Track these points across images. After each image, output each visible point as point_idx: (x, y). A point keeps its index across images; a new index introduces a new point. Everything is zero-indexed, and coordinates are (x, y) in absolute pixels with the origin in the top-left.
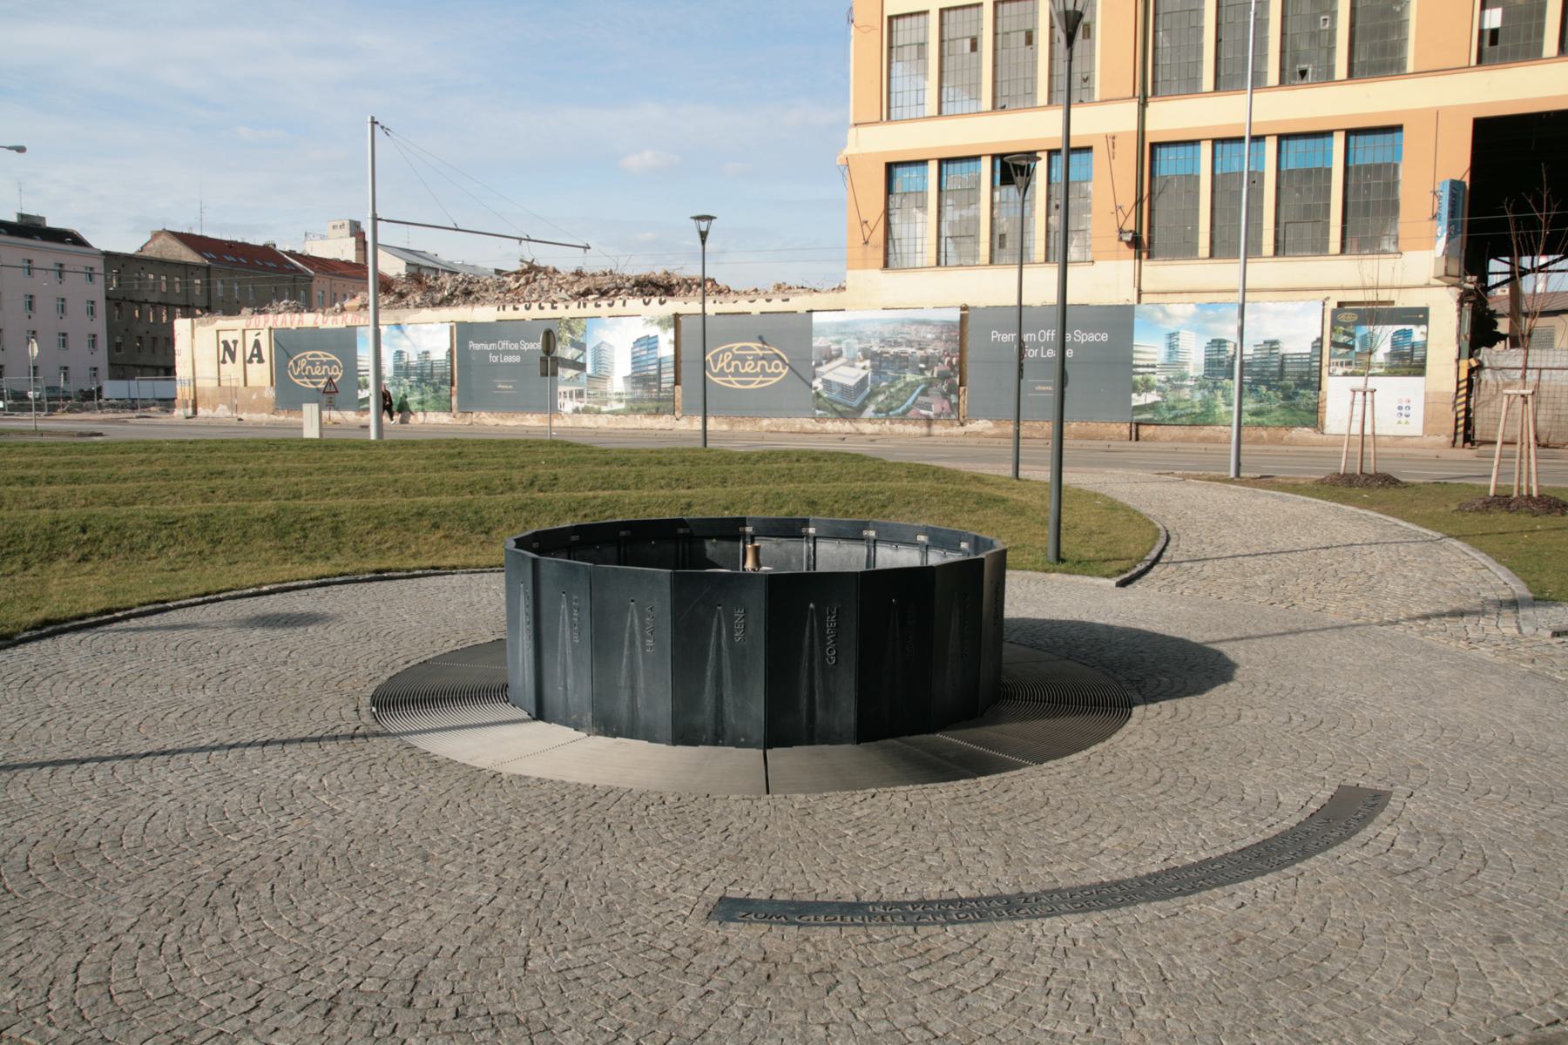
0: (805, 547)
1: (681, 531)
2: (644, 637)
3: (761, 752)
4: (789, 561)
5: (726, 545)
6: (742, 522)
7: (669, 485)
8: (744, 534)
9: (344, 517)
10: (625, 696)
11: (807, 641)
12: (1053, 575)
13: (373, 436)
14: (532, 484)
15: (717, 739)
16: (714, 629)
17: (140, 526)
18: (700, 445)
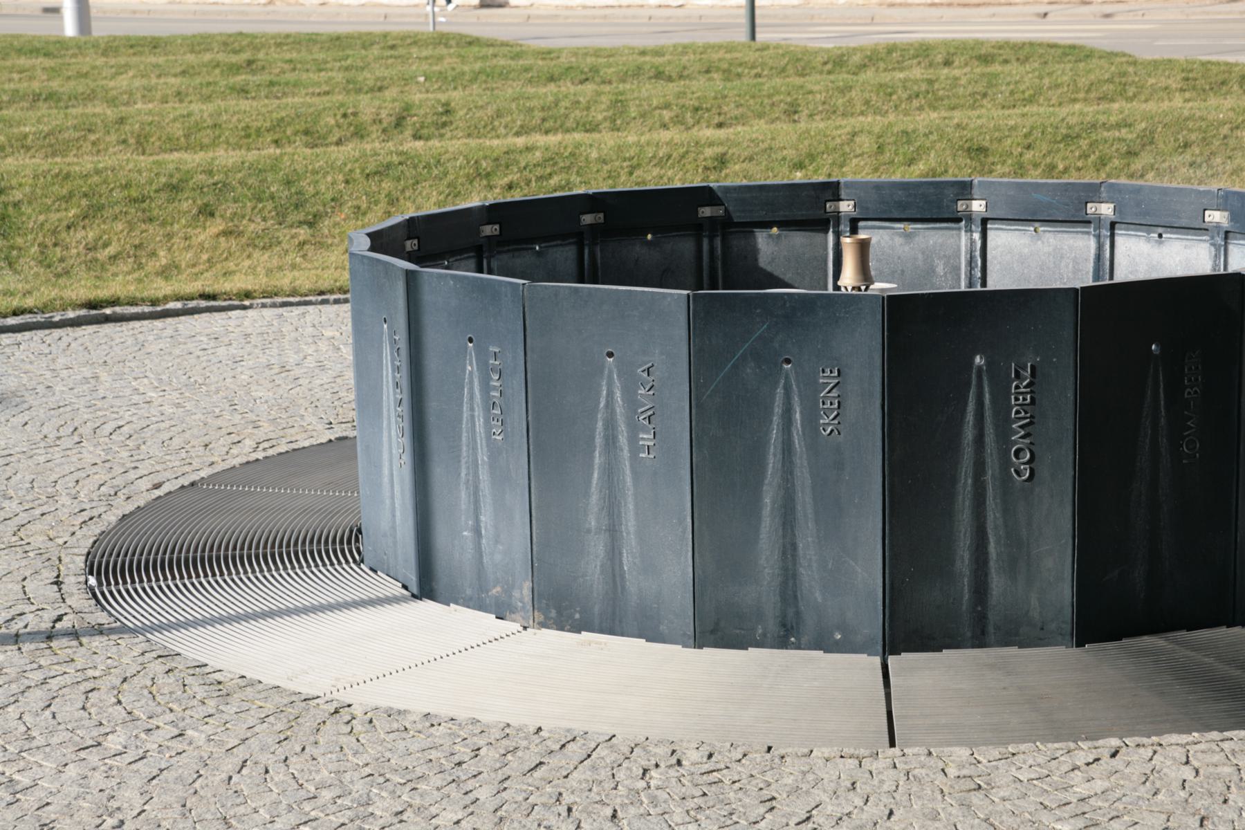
0: (963, 240)
1: (706, 212)
2: (634, 429)
3: (877, 660)
4: (931, 271)
5: (798, 239)
6: (832, 190)
7: (678, 120)
8: (837, 216)
9: (17, 195)
10: (597, 548)
11: (969, 434)
13: (70, 28)
14: (399, 123)
15: (786, 635)
16: (778, 410)
18: (742, 36)
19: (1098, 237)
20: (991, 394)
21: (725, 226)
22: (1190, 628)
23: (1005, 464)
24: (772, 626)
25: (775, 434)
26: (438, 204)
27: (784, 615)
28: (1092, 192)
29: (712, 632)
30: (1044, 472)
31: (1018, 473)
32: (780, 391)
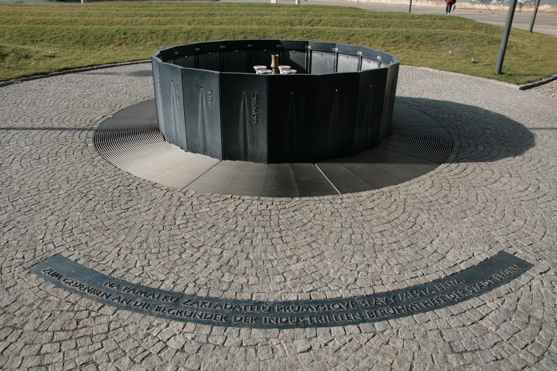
1: (278, 46)
2: (176, 100)
4: (326, 63)
5: (299, 54)
6: (307, 43)
7: (365, 26)
11: (242, 110)
12: (491, 81)
13: (296, 3)
14: (309, 23)
16: (200, 99)
17: (143, 33)
18: (408, 11)
22: (300, 162)
23: (251, 118)
24: (201, 149)
25: (200, 104)
28: (359, 49)
30: (260, 121)
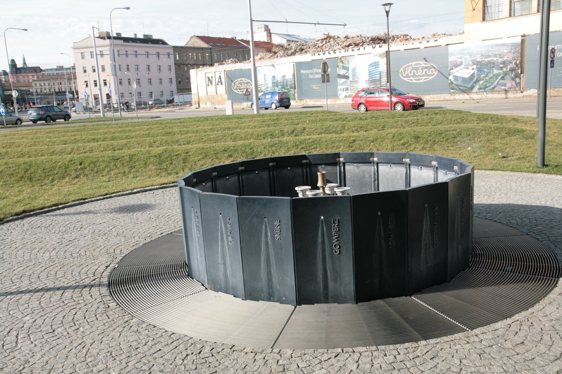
0: (372, 168)
1: (304, 161)
2: (227, 236)
3: (293, 307)
4: (364, 176)
5: (329, 168)
6: (338, 155)
7: (357, 130)
8: (339, 162)
9: (190, 153)
10: (221, 268)
11: (320, 240)
12: (539, 175)
14: (292, 132)
15: (270, 298)
16: (264, 232)
17: (104, 161)
19: (406, 168)
20: (326, 228)
21: (310, 165)
22: (394, 297)
23: (332, 249)
24: (266, 294)
25: (263, 239)
26: (284, 153)
27: (269, 292)
28: (404, 156)
29: (250, 295)
30: (343, 251)
31: (336, 252)
32: (264, 226)
